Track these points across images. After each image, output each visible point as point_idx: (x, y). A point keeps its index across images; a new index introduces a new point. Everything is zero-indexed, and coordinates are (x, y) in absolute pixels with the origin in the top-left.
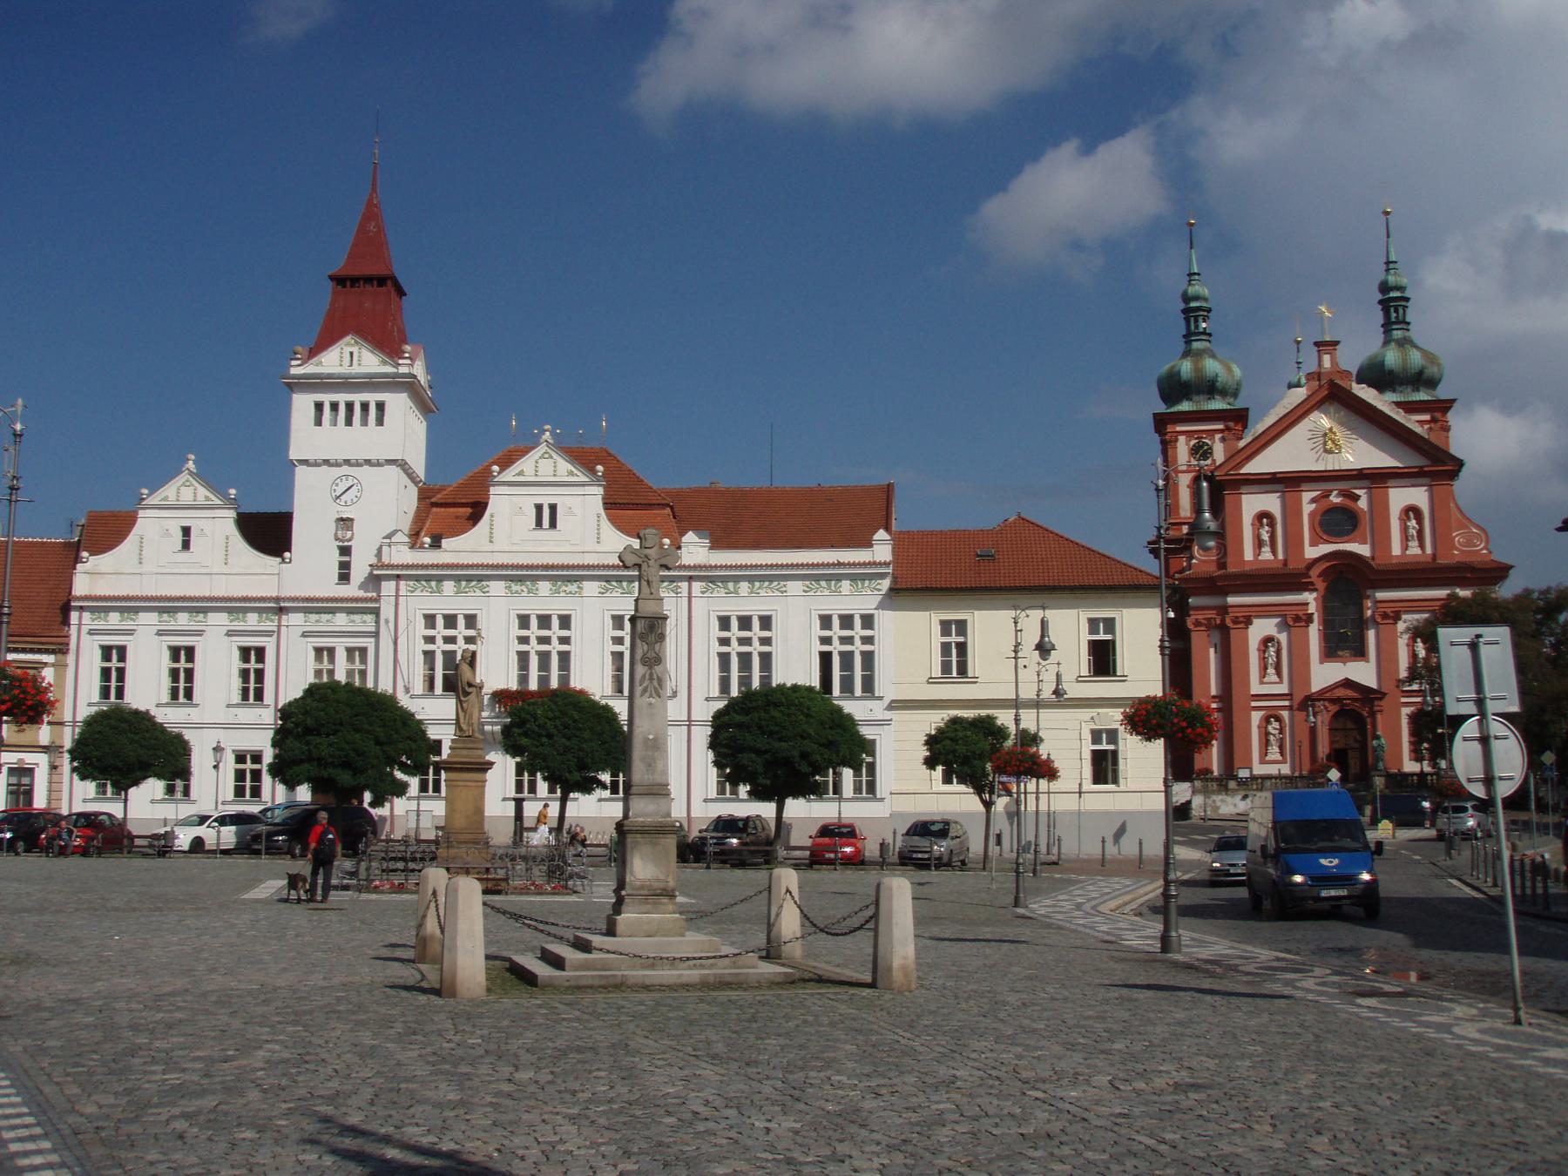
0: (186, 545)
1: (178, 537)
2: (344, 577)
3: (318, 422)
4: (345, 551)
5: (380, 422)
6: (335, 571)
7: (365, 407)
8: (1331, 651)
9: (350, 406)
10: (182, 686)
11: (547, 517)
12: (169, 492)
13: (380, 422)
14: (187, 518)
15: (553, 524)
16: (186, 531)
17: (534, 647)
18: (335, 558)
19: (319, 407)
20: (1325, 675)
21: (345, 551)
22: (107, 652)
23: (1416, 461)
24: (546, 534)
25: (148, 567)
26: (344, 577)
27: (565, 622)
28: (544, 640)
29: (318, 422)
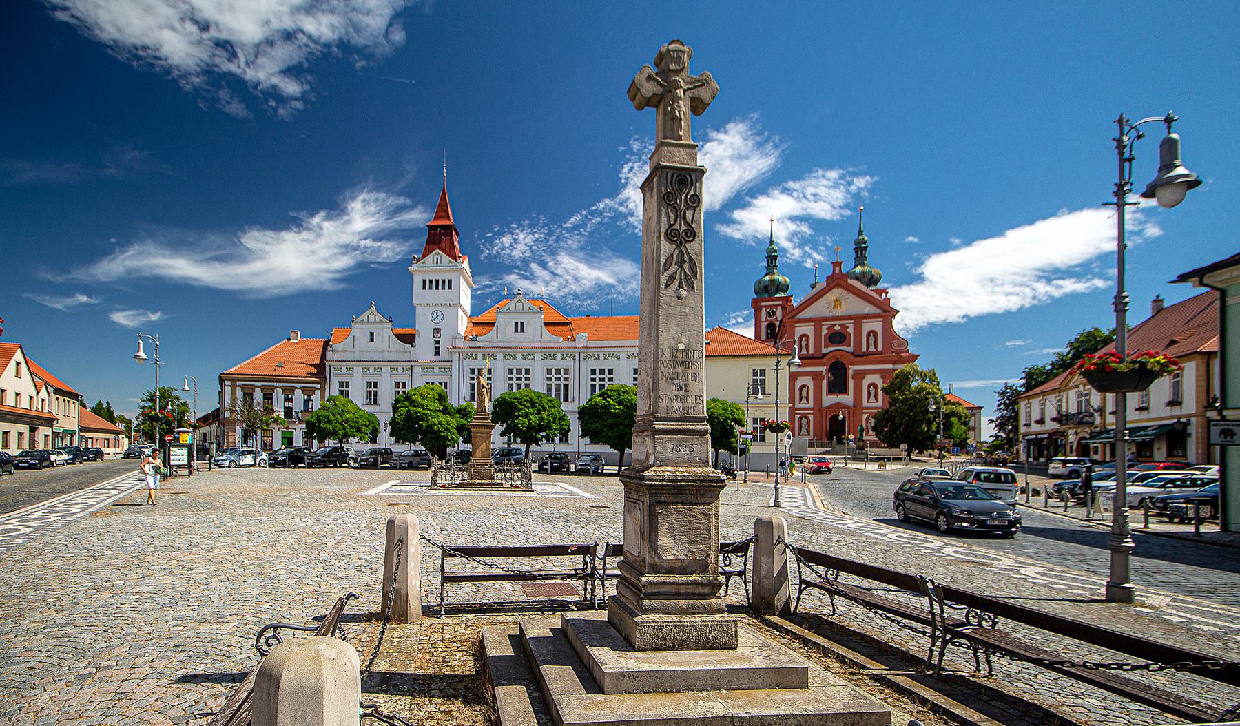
0: (372, 340)
2: (437, 353)
3: (424, 288)
4: (437, 342)
5: (450, 288)
7: (443, 281)
8: (830, 392)
9: (437, 281)
10: (373, 399)
11: (520, 327)
12: (364, 317)
13: (450, 288)
15: (522, 330)
16: (372, 334)
18: (433, 345)
19: (424, 282)
20: (828, 400)
21: (437, 342)
22: (341, 384)
23: (876, 311)
24: (519, 334)
26: (437, 353)
27: (527, 371)
28: (518, 379)
29: (424, 288)
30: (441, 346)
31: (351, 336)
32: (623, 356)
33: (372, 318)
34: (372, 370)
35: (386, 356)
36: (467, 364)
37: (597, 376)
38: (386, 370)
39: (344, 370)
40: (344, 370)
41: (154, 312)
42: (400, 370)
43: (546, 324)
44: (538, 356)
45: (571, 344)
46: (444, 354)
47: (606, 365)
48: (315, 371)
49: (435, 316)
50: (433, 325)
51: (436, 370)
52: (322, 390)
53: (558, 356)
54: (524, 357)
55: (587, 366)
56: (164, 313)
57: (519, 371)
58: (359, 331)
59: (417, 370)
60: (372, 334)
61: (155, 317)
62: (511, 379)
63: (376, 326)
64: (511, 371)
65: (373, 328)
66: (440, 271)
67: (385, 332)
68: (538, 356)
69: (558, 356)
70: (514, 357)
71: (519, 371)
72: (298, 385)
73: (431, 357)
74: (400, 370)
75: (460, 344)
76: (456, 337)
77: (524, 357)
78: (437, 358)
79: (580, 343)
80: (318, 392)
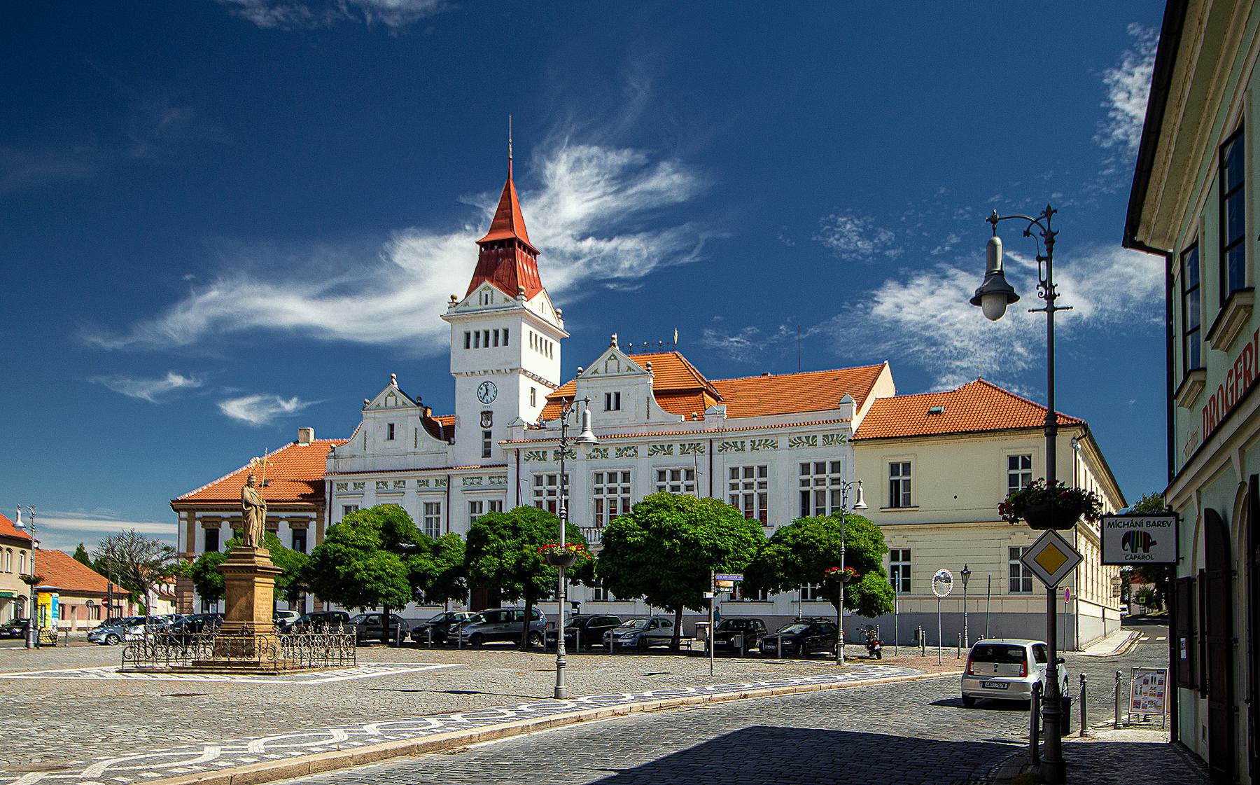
0: (391, 437)
1: (385, 432)
2: (487, 454)
4: (488, 435)
6: (480, 449)
14: (391, 417)
17: (605, 496)
21: (488, 435)
25: (369, 451)
26: (487, 454)
30: (493, 440)
31: (361, 433)
32: (783, 442)
33: (391, 401)
34: (391, 485)
35: (412, 462)
36: (529, 469)
37: (741, 480)
38: (412, 483)
39: (351, 487)
40: (351, 487)
41: (287, 398)
42: (432, 483)
43: (659, 394)
44: (643, 450)
45: (695, 425)
46: (497, 456)
47: (753, 459)
48: (310, 491)
49: (485, 391)
50: (481, 407)
51: (485, 481)
52: (320, 520)
53: (676, 448)
54: (620, 453)
55: (724, 462)
56: (303, 398)
57: (612, 478)
58: (372, 424)
59: (457, 482)
60: (392, 426)
61: (290, 406)
62: (599, 491)
63: (395, 413)
64: (599, 477)
65: (391, 417)
66: (490, 316)
67: (410, 420)
68: (643, 450)
69: (676, 448)
70: (604, 454)
71: (612, 478)
72: (283, 515)
73: (477, 459)
74: (432, 483)
75: (518, 436)
76: (515, 423)
77: (620, 453)
78: (487, 461)
79: (711, 424)
80: (313, 525)
